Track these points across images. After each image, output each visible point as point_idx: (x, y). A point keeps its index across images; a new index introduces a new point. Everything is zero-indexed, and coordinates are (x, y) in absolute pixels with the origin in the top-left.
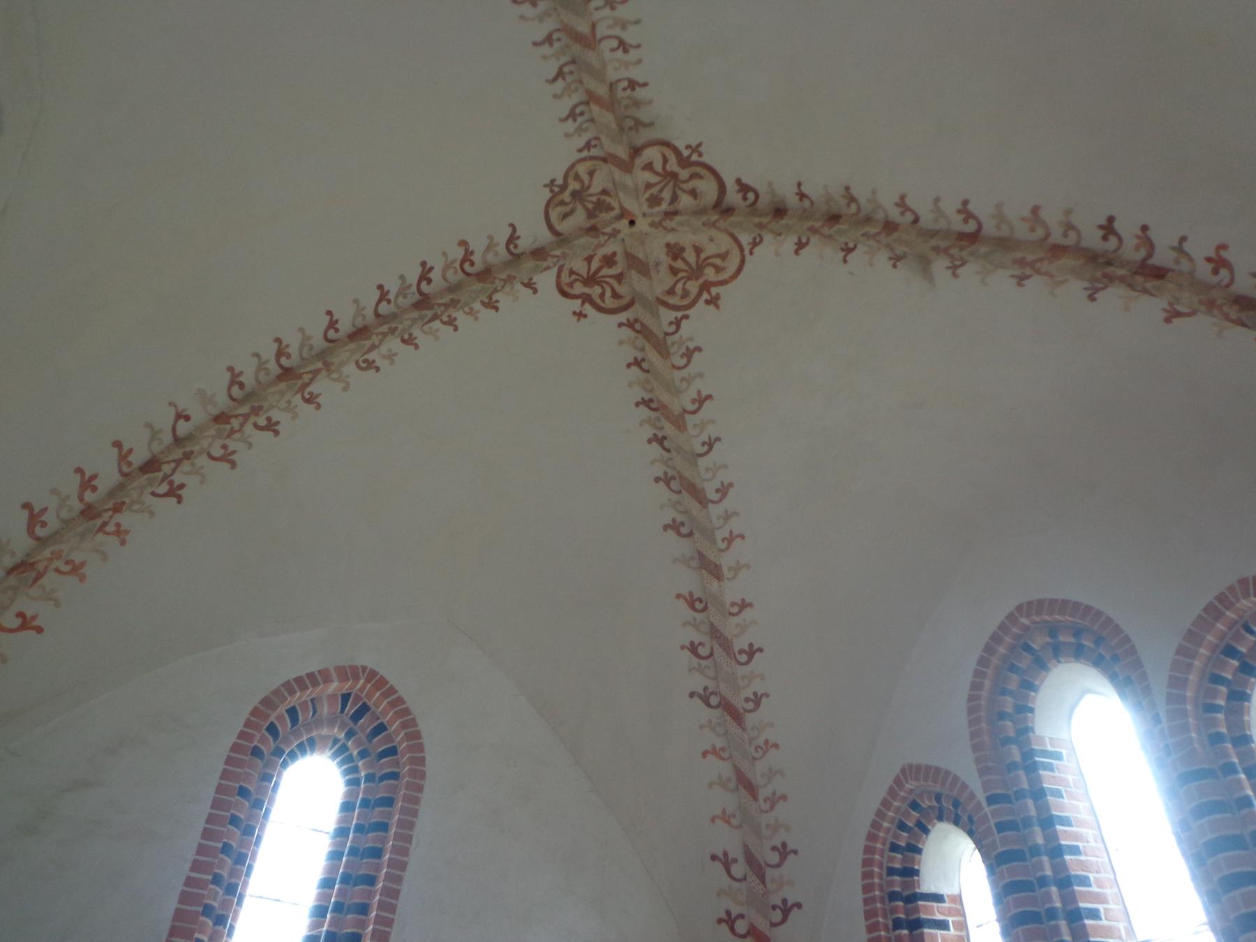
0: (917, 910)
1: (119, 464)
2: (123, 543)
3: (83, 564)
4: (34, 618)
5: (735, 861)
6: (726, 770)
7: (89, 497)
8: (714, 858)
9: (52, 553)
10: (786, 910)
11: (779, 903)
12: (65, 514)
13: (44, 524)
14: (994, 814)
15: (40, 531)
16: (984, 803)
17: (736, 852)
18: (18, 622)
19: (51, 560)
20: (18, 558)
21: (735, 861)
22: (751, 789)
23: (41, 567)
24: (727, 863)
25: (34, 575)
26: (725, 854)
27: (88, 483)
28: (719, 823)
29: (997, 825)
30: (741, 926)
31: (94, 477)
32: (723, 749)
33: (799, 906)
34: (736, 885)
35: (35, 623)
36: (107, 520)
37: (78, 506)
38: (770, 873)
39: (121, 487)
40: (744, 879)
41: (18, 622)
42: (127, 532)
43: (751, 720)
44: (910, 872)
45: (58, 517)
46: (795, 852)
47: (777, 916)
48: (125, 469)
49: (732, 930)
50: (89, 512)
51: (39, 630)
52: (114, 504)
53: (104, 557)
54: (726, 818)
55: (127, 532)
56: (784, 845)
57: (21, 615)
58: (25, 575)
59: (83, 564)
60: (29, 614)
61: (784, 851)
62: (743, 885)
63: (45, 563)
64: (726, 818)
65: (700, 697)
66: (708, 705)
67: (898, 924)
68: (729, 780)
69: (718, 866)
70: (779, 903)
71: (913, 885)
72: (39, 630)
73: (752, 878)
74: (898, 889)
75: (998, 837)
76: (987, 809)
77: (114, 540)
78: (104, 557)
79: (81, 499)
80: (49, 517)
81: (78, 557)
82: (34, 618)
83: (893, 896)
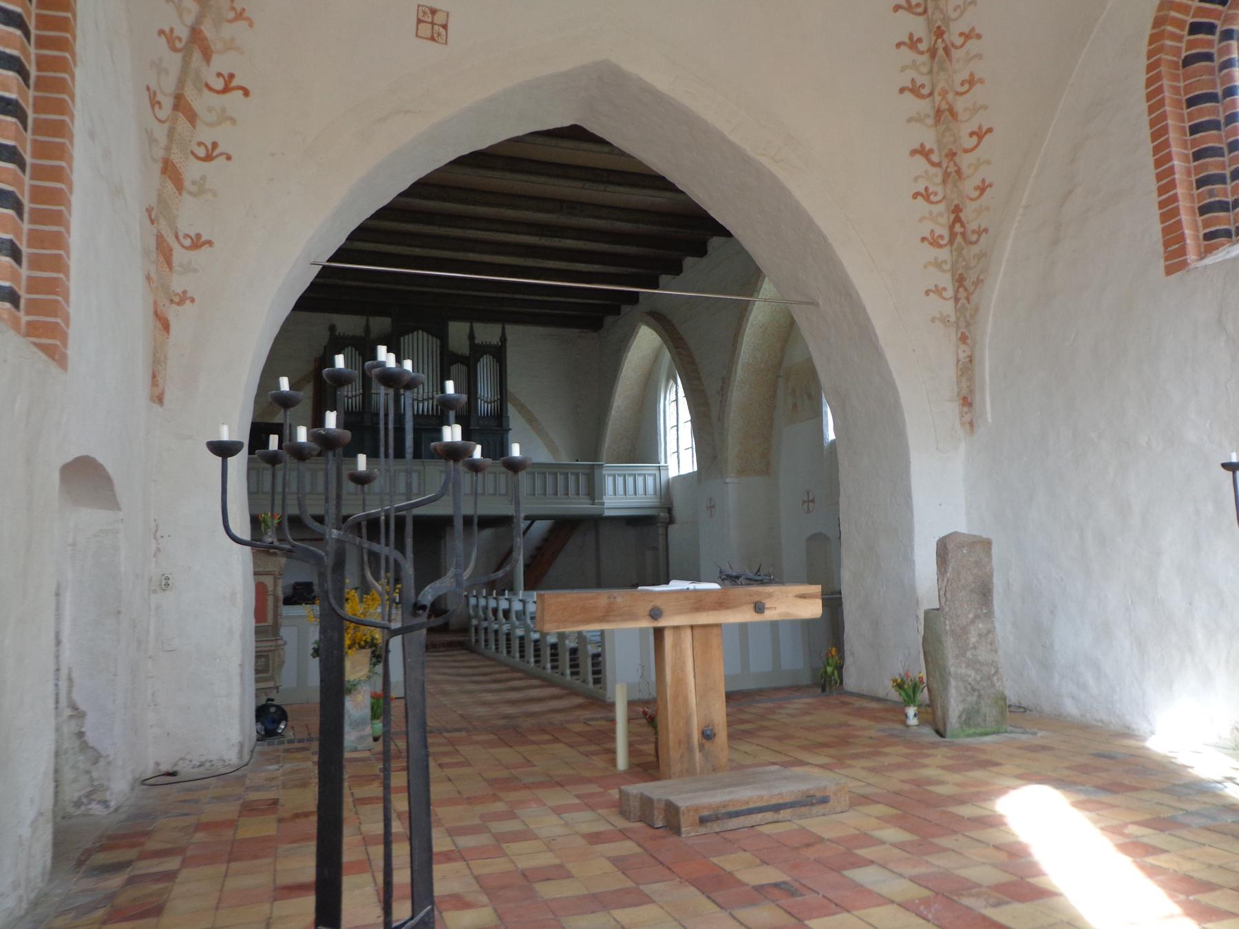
1: (913, 13)
2: (979, 36)
3: (972, 75)
4: (980, 127)
7: (923, 47)
9: (940, 95)
12: (925, 70)
13: (923, 86)
15: (925, 91)
18: (975, 139)
19: (944, 98)
20: (932, 113)
23: (944, 106)
25: (947, 113)
27: (913, 43)
31: (911, 36)
35: (984, 130)
36: (944, 46)
37: (925, 58)
39: (930, 22)
41: (975, 139)
42: (973, 30)
45: (924, 74)
48: (920, 10)
50: (933, 52)
51: (990, 130)
52: (934, 35)
53: (979, 56)
55: (973, 30)
57: (972, 134)
58: (942, 119)
59: (972, 75)
60: (975, 129)
63: (944, 102)
72: (990, 130)
77: (972, 45)
78: (979, 56)
79: (922, 53)
80: (920, 80)
81: (965, 75)
82: (980, 127)
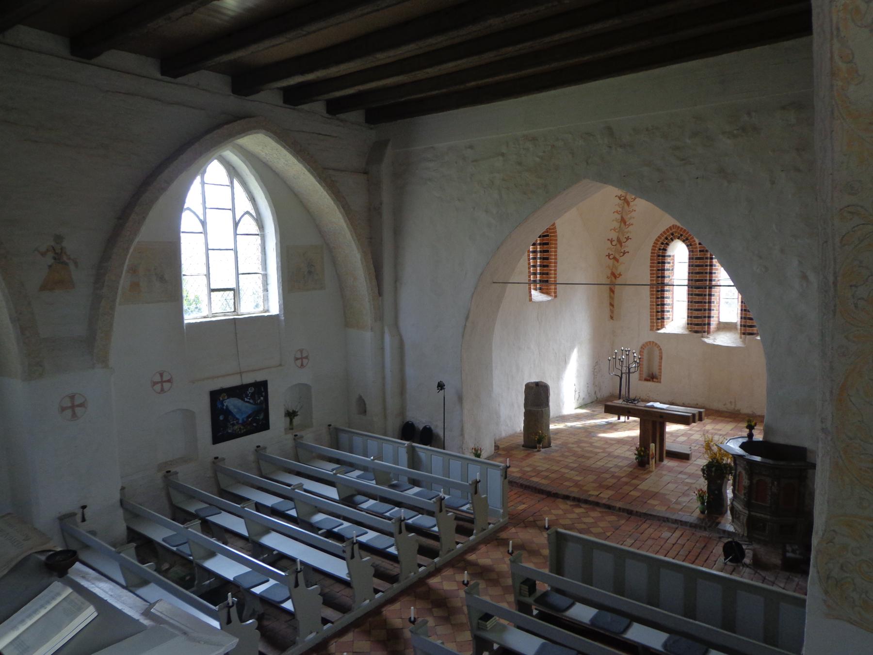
0: (665, 259)
5: (614, 241)
6: (619, 217)
8: (608, 240)
10: (624, 253)
11: (623, 251)
14: (700, 248)
16: (698, 244)
17: (615, 238)
21: (614, 241)
22: (625, 223)
24: (612, 241)
26: (612, 239)
28: (612, 230)
29: (700, 250)
30: (611, 257)
32: (620, 211)
33: (628, 252)
34: (613, 247)
38: (623, 244)
40: (616, 245)
43: (632, 204)
44: (665, 250)
46: (630, 239)
47: (622, 254)
49: (609, 258)
54: (614, 229)
56: (628, 237)
61: (628, 239)
62: (615, 247)
64: (614, 229)
65: (619, 197)
66: (620, 199)
67: (659, 263)
68: (619, 219)
69: (609, 242)
70: (623, 251)
71: (665, 253)
73: (618, 246)
74: (661, 254)
75: (699, 253)
76: (698, 246)
83: (659, 256)
